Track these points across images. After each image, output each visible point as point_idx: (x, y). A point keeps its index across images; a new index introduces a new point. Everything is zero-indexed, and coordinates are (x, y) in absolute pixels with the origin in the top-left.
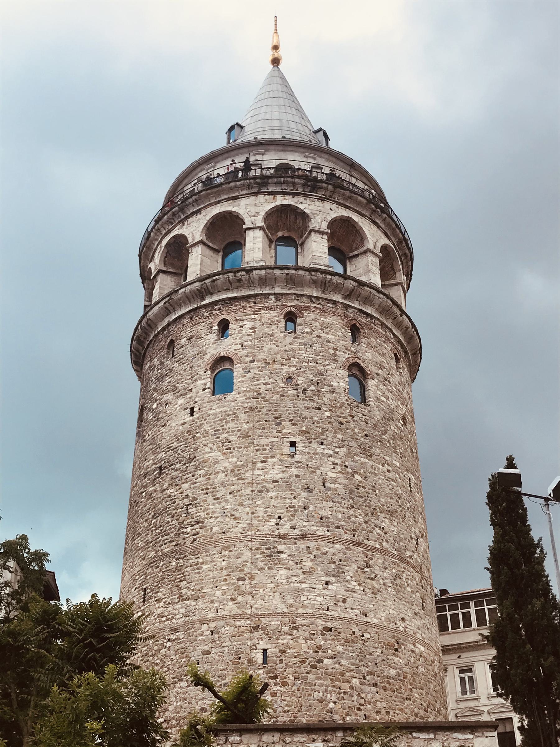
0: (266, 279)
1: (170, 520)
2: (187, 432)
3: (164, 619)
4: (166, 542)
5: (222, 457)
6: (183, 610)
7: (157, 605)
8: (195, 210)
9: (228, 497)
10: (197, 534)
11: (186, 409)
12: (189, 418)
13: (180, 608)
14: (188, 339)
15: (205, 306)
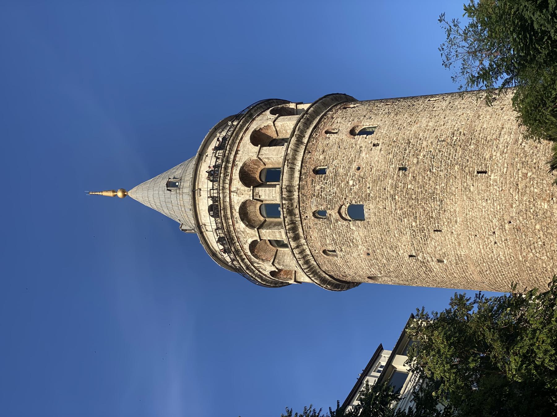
0: (316, 110)
1: (441, 153)
2: (388, 146)
3: (505, 150)
4: (454, 155)
5: (418, 125)
6: (506, 136)
7: (494, 157)
8: (234, 154)
9: (447, 119)
10: (461, 133)
11: (372, 148)
12: (379, 147)
13: (505, 138)
14: (323, 153)
15: (308, 142)
